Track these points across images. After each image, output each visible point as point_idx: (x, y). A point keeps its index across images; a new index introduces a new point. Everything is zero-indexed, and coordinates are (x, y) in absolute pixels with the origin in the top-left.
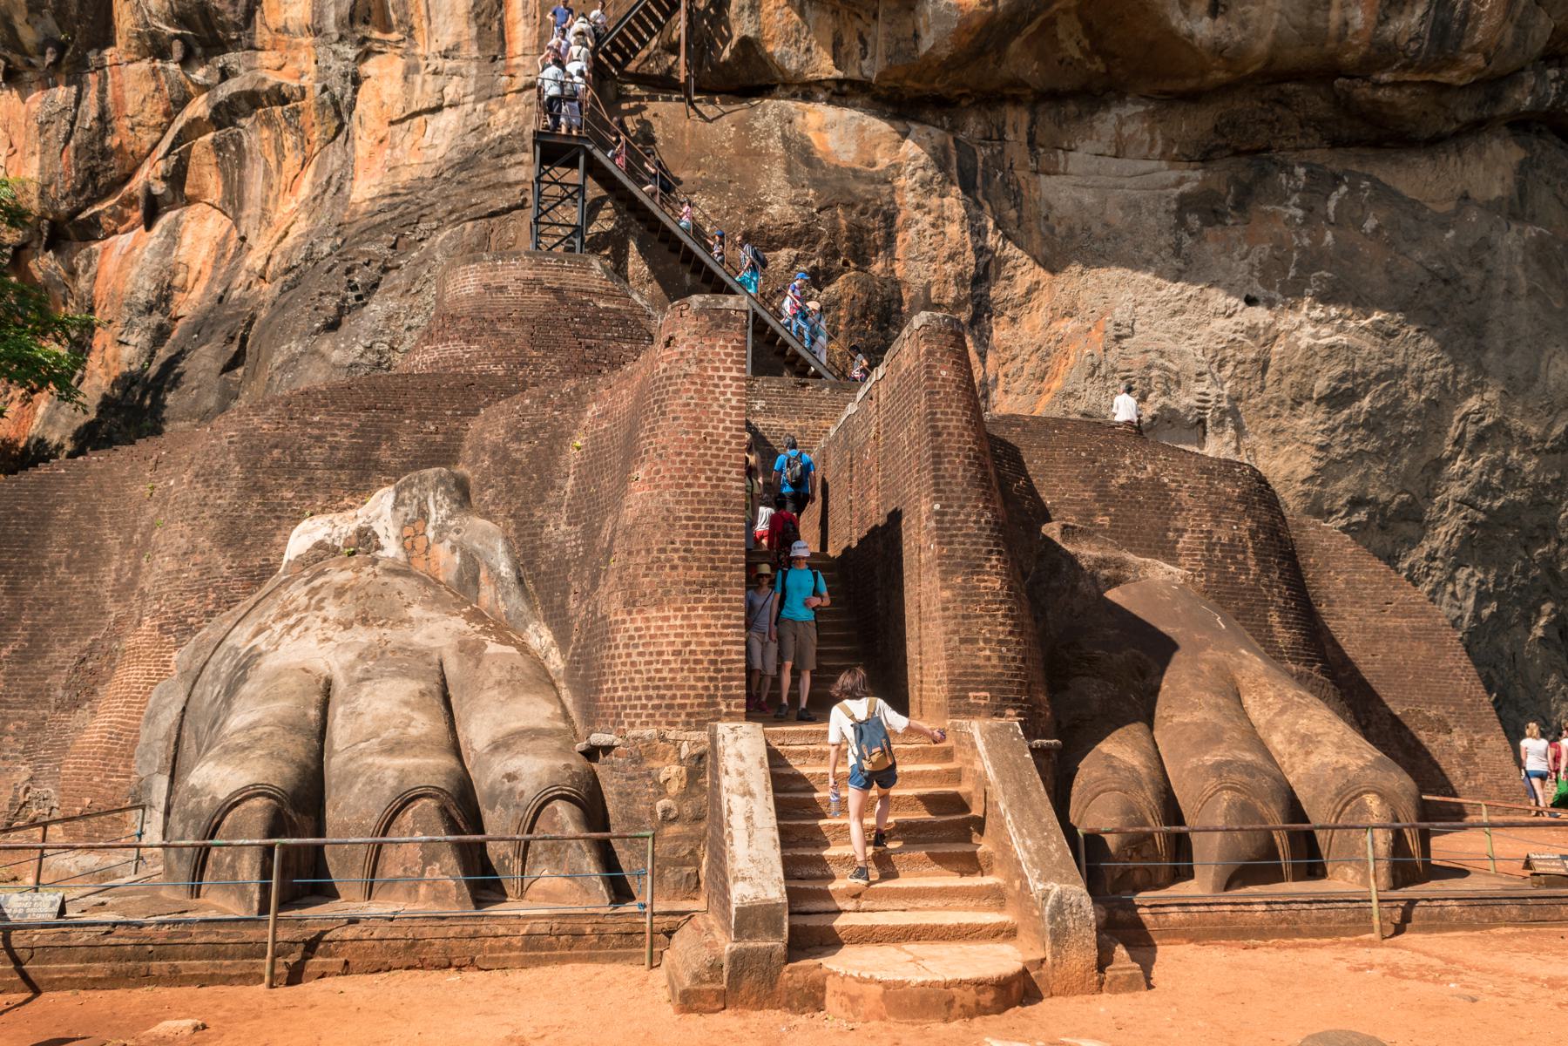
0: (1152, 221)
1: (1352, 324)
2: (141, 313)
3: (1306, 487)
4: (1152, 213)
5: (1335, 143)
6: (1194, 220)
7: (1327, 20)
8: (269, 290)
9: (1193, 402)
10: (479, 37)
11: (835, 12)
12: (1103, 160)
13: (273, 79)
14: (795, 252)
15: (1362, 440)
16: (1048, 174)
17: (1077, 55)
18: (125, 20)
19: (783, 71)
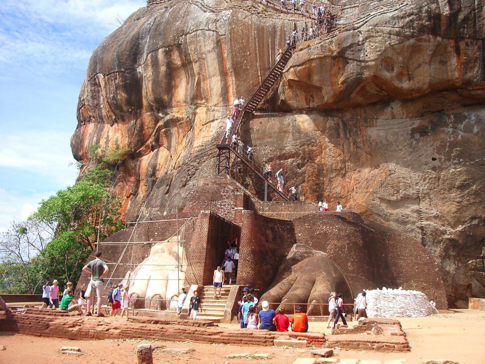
0: (402, 138)
1: (468, 163)
2: (149, 177)
3: (455, 215)
4: (402, 135)
5: (465, 106)
6: (417, 136)
7: (448, 76)
8: (175, 172)
9: (414, 192)
10: (223, 100)
11: (305, 91)
12: (387, 120)
13: (177, 115)
14: (293, 159)
15: (474, 199)
16: (370, 127)
17: (376, 93)
18: (145, 102)
19: (293, 107)
